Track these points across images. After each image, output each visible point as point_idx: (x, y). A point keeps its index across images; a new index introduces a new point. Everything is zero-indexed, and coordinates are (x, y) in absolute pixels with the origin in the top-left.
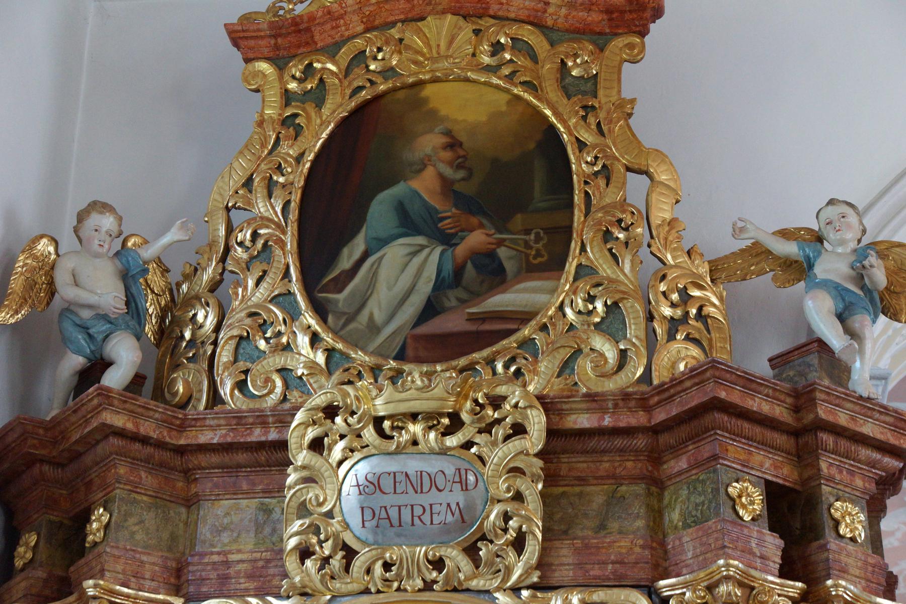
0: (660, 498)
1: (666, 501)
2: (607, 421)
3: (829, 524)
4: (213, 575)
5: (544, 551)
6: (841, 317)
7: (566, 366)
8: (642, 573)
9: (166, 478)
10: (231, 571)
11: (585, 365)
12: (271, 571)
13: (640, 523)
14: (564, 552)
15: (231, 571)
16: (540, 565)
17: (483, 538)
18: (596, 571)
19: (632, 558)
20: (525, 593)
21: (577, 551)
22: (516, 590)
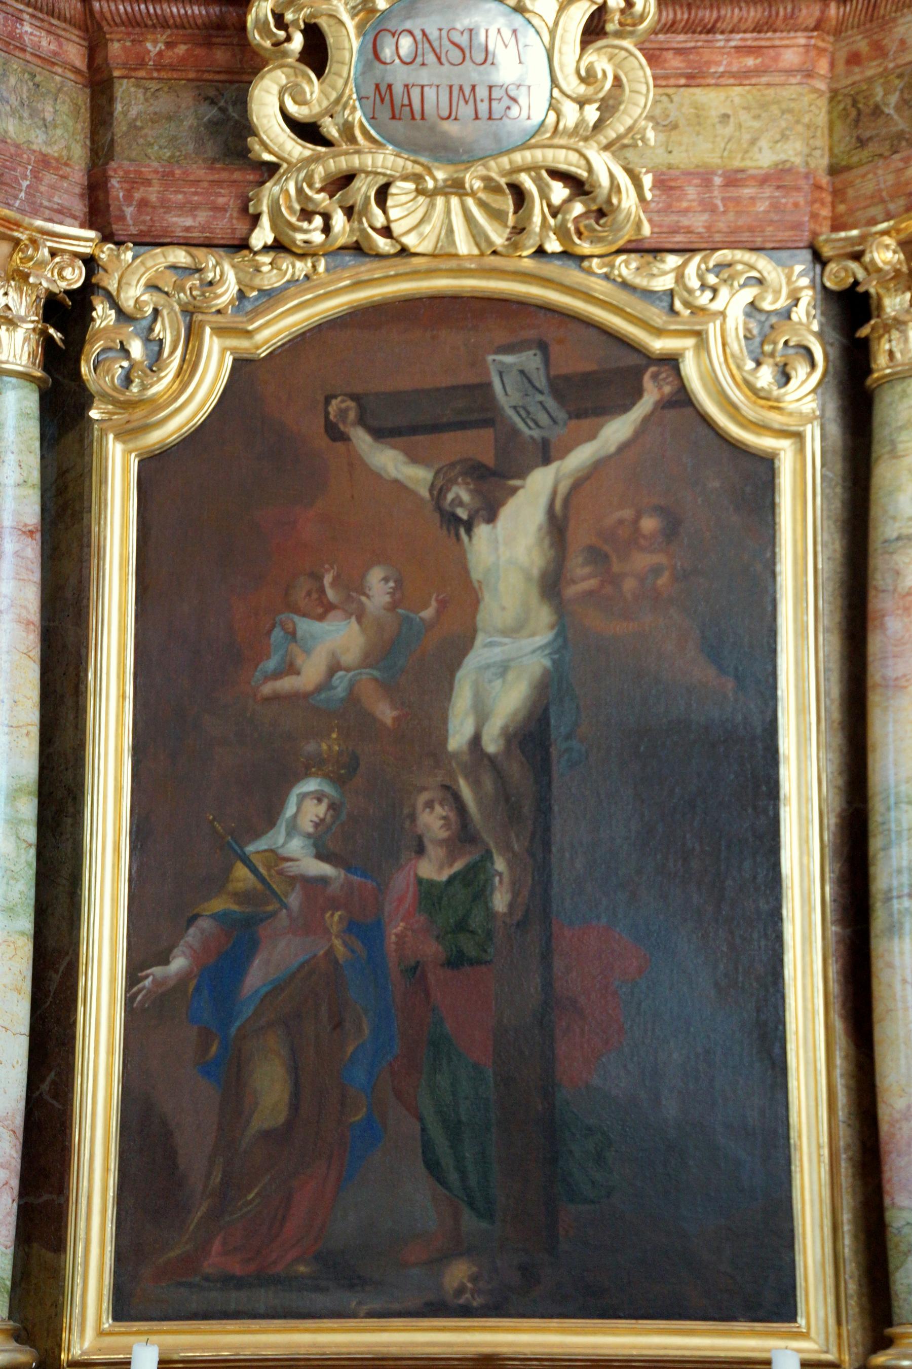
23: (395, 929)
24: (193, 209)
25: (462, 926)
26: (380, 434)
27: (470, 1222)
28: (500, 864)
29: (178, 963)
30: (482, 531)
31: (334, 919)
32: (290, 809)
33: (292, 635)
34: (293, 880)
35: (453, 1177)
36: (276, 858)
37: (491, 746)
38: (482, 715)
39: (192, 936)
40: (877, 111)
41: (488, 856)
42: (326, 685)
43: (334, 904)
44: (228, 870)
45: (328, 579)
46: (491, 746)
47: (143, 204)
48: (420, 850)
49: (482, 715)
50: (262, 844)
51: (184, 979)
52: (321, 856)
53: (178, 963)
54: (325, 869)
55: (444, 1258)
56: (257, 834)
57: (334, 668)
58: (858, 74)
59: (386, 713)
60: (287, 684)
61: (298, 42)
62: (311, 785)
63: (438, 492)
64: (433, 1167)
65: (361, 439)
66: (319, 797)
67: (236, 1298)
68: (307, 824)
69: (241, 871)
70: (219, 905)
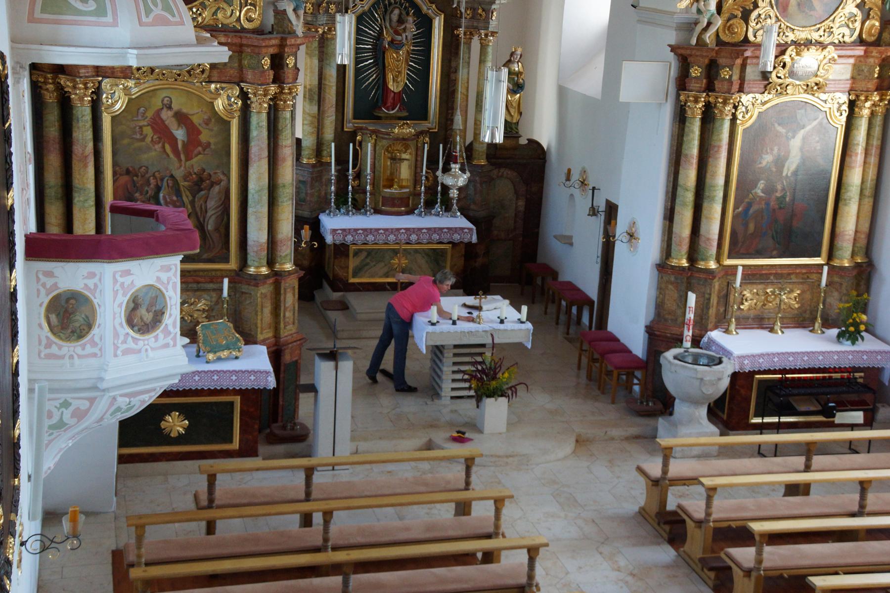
0: (241, 56)
1: (243, 56)
2: (229, 40)
3: (286, 65)
4: (110, 71)
5: (210, 72)
6: (294, 10)
7: (215, 13)
8: (237, 80)
9: (279, 345)
10: (115, 70)
11: (220, 15)
12: (128, 71)
13: (236, 65)
14: (215, 72)
15: (115, 70)
16: (209, 77)
17: (192, 69)
18: (224, 78)
19: (233, 76)
20: (204, 83)
21: (218, 73)
22: (201, 83)
23: (772, 203)
24: (756, 88)
25: (781, 203)
26: (779, 124)
27: (777, 246)
28: (788, 194)
29: (740, 209)
30: (792, 140)
31: (763, 202)
32: (759, 185)
33: (762, 157)
34: (758, 196)
35: (776, 239)
36: (756, 193)
37: (789, 175)
38: (788, 169)
39: (743, 205)
40: (863, 70)
41: (786, 193)
42: (766, 166)
43: (763, 200)
44: (748, 195)
45: (768, 148)
46: (789, 175)
47: (749, 87)
48: (777, 192)
49: (788, 169)
50: (754, 191)
51: (741, 211)
52: (763, 193)
53: (740, 209)
54: (763, 195)
55: (773, 250)
56: (754, 189)
57: (768, 162)
58: (860, 63)
59: (774, 169)
60: (760, 166)
61: (782, 64)
62: (762, 182)
63: (787, 133)
64: (773, 238)
65: (776, 125)
66: (763, 183)
67: (744, 256)
68: (761, 188)
69: (751, 195)
70: (747, 200)
